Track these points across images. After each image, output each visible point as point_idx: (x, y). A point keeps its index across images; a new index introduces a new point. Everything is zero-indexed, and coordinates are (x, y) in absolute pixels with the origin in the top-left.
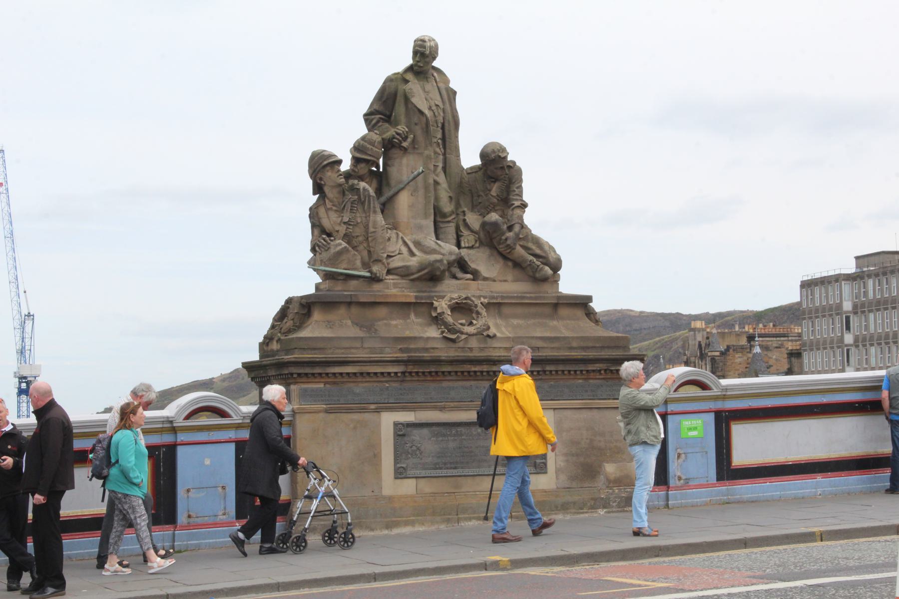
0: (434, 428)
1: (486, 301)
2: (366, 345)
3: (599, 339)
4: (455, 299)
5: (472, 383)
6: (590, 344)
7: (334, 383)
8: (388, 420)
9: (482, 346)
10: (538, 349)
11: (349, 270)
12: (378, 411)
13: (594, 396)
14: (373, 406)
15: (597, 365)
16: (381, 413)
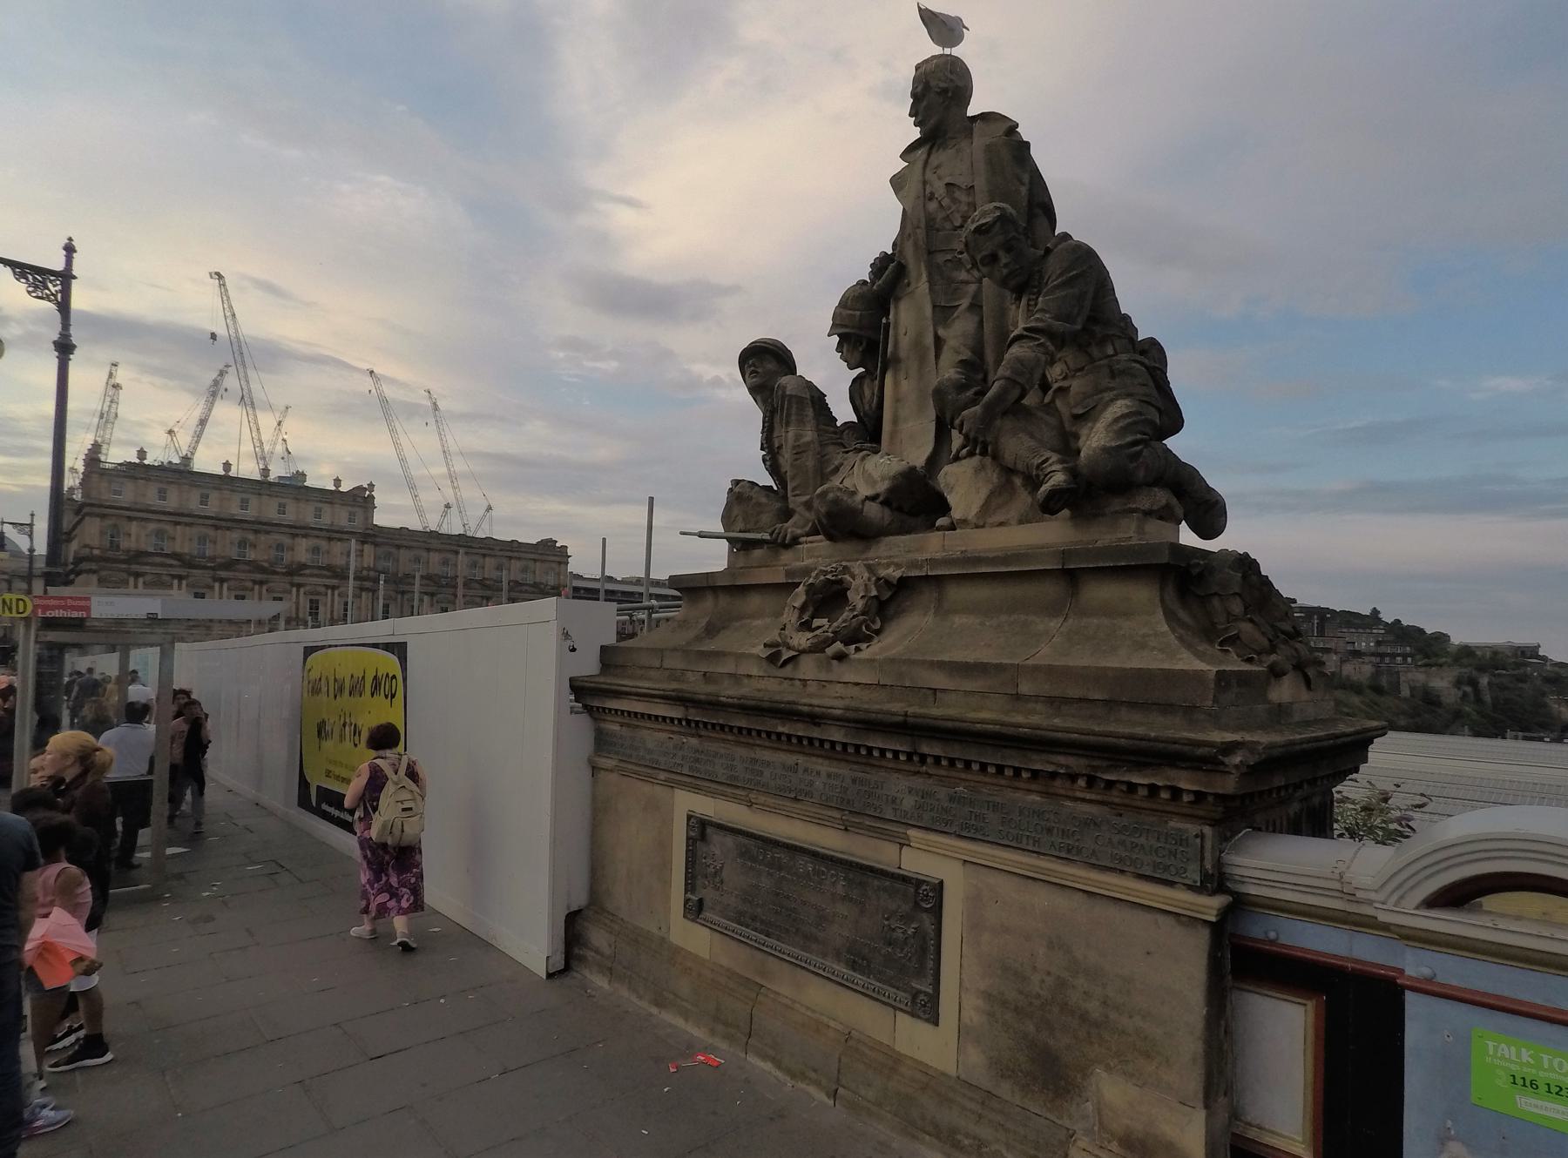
0: (741, 839)
1: (898, 574)
2: (668, 663)
3: (1098, 676)
4: (826, 573)
5: (801, 759)
6: (1074, 692)
7: (628, 725)
8: (688, 802)
9: (823, 676)
10: (935, 694)
11: (749, 531)
12: (671, 785)
13: (1069, 851)
14: (663, 776)
15: (1062, 759)
16: (676, 790)
